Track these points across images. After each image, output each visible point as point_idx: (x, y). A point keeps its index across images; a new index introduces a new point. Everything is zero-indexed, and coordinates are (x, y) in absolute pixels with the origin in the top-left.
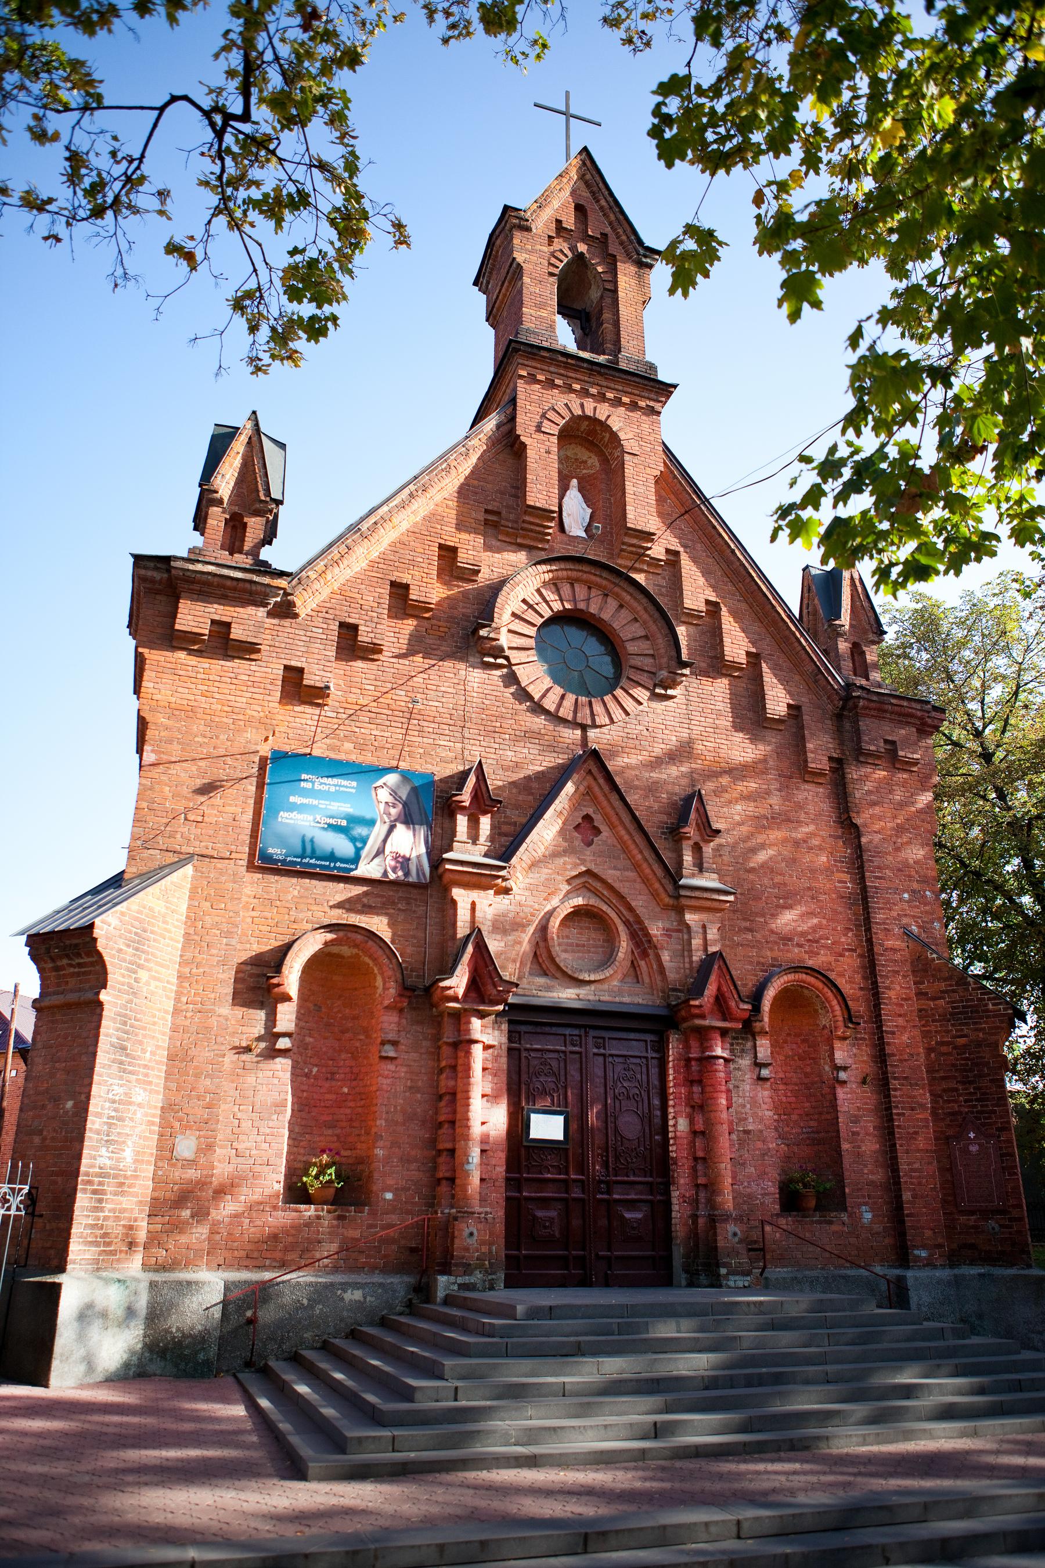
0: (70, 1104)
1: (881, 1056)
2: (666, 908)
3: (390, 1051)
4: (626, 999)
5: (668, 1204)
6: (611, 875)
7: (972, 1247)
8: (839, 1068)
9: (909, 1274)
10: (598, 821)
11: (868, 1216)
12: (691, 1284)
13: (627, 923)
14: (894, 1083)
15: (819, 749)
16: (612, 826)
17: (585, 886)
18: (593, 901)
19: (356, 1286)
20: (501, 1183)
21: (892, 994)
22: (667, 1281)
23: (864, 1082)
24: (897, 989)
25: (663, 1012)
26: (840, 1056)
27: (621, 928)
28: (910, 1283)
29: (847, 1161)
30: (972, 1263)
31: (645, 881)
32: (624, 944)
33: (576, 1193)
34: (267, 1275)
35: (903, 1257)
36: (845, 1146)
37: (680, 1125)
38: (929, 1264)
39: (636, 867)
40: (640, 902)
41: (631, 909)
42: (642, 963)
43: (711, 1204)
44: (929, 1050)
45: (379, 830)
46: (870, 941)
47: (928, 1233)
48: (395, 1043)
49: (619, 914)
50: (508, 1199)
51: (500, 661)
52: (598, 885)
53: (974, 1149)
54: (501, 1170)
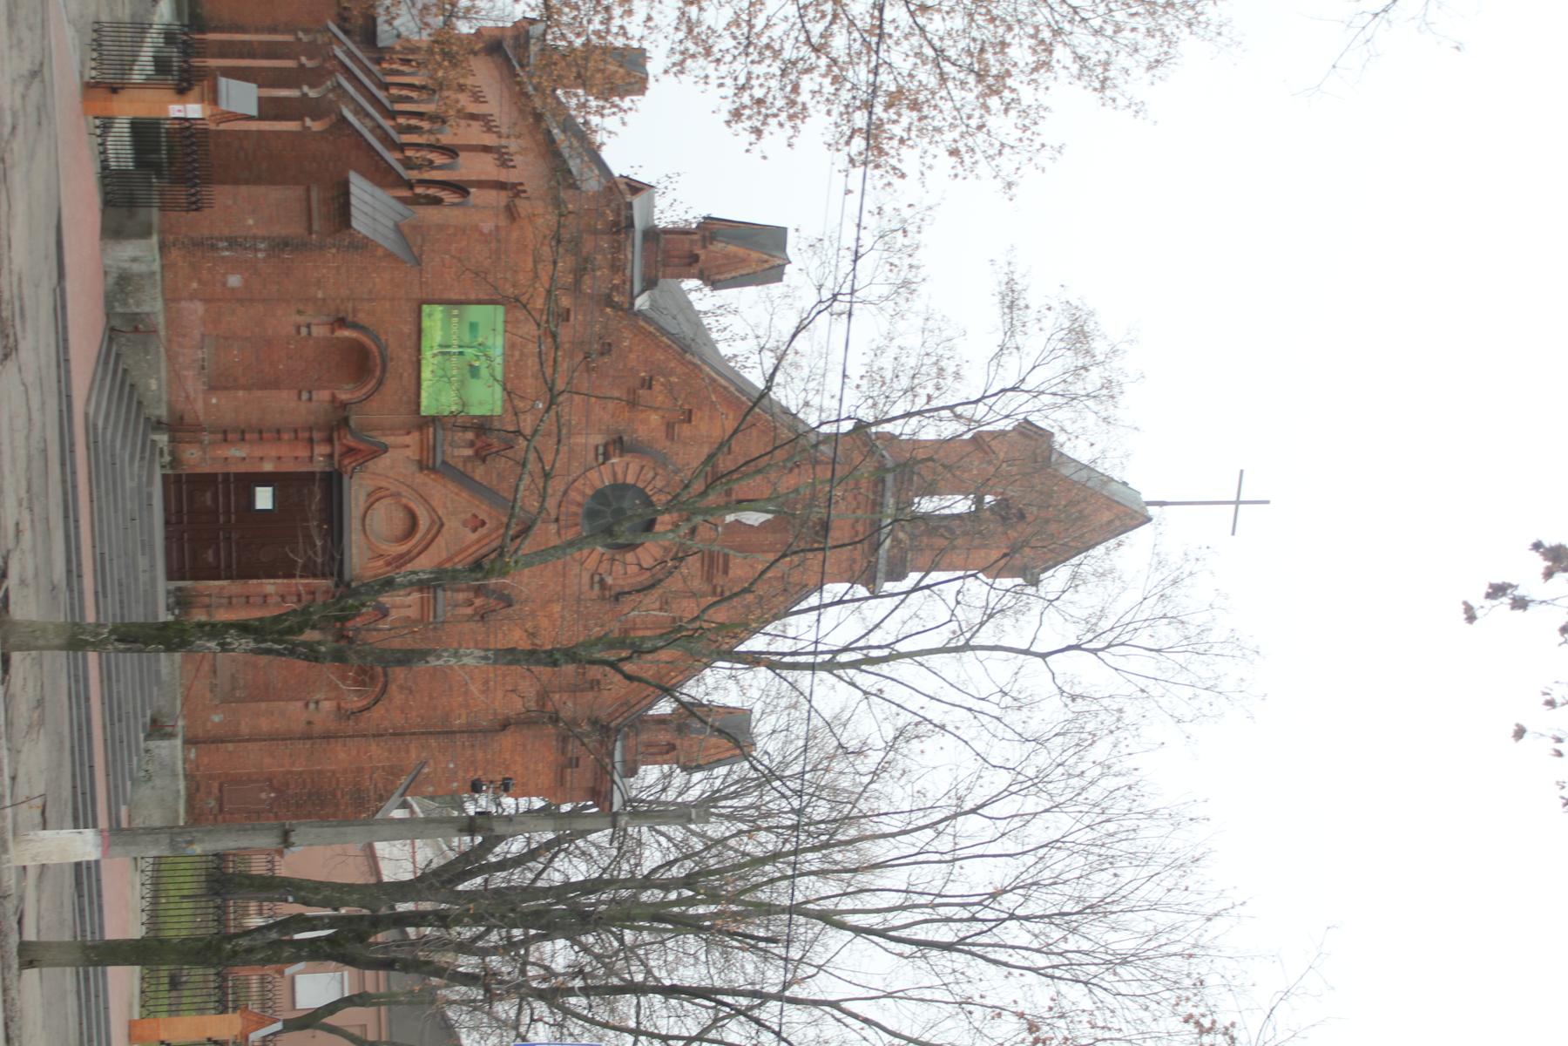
0: (251, 222)
3: (305, 396)
4: (354, 551)
5: (219, 578)
6: (441, 541)
7: (198, 790)
8: (317, 702)
9: (178, 742)
10: (482, 531)
11: (217, 718)
12: (168, 592)
13: (409, 552)
14: (308, 744)
16: (479, 541)
19: (159, 387)
20: (225, 470)
21: (374, 747)
22: (170, 576)
23: (309, 723)
25: (347, 577)
27: (404, 548)
28: (172, 742)
29: (253, 705)
30: (187, 789)
33: (222, 519)
34: (162, 333)
36: (263, 705)
38: (185, 760)
41: (420, 553)
42: (381, 562)
43: (219, 606)
44: (334, 772)
47: (206, 760)
48: (310, 399)
49: (415, 546)
50: (216, 475)
51: (601, 459)
52: (434, 531)
53: (263, 796)
54: (233, 469)
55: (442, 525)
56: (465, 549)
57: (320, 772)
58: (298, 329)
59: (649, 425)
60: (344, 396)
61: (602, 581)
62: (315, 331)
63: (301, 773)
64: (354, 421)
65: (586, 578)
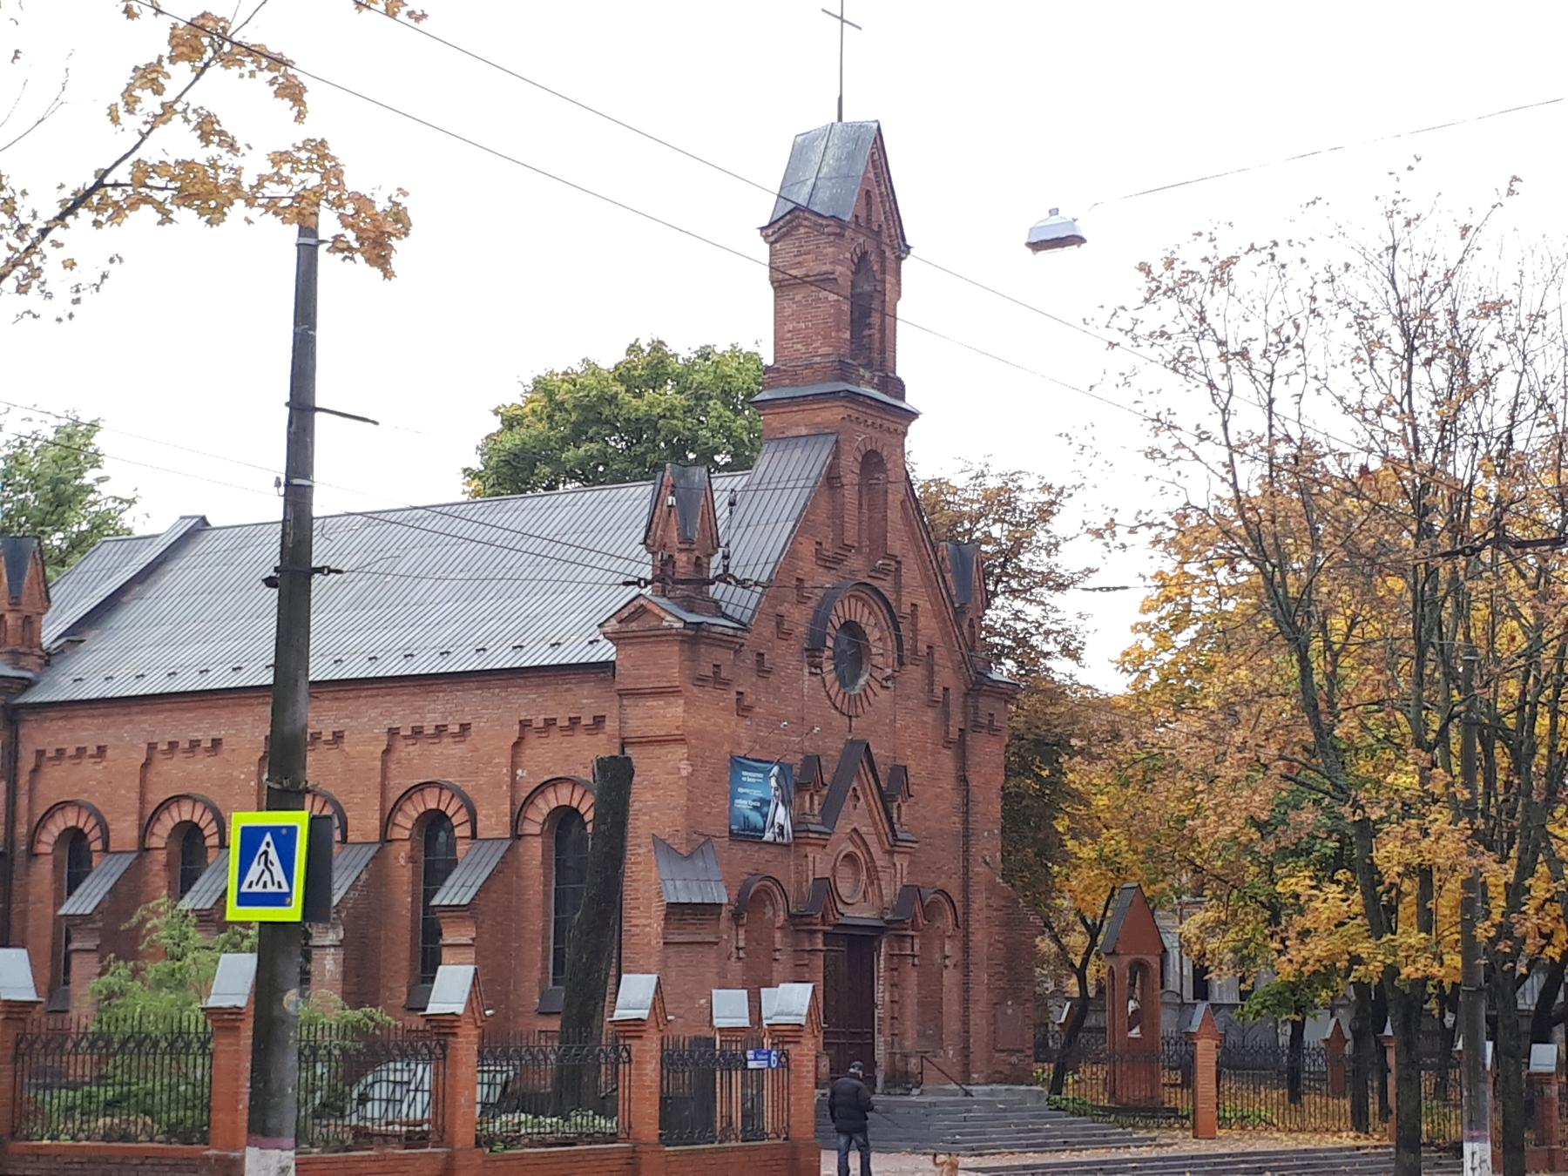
1: (966, 950)
2: (887, 852)
3: (778, 955)
6: (863, 830)
10: (859, 793)
14: (971, 967)
16: (866, 796)
18: (852, 848)
24: (979, 901)
25: (880, 924)
30: (1001, 1082)
31: (878, 835)
32: (864, 877)
35: (966, 1078)
37: (881, 994)
39: (875, 824)
40: (875, 849)
44: (990, 945)
45: (772, 806)
46: (966, 868)
53: (1010, 1011)
55: (855, 830)
56: (870, 811)
58: (739, 958)
59: (799, 617)
60: (781, 918)
61: (887, 679)
62: (741, 944)
63: (990, 976)
64: (793, 911)
65: (883, 694)
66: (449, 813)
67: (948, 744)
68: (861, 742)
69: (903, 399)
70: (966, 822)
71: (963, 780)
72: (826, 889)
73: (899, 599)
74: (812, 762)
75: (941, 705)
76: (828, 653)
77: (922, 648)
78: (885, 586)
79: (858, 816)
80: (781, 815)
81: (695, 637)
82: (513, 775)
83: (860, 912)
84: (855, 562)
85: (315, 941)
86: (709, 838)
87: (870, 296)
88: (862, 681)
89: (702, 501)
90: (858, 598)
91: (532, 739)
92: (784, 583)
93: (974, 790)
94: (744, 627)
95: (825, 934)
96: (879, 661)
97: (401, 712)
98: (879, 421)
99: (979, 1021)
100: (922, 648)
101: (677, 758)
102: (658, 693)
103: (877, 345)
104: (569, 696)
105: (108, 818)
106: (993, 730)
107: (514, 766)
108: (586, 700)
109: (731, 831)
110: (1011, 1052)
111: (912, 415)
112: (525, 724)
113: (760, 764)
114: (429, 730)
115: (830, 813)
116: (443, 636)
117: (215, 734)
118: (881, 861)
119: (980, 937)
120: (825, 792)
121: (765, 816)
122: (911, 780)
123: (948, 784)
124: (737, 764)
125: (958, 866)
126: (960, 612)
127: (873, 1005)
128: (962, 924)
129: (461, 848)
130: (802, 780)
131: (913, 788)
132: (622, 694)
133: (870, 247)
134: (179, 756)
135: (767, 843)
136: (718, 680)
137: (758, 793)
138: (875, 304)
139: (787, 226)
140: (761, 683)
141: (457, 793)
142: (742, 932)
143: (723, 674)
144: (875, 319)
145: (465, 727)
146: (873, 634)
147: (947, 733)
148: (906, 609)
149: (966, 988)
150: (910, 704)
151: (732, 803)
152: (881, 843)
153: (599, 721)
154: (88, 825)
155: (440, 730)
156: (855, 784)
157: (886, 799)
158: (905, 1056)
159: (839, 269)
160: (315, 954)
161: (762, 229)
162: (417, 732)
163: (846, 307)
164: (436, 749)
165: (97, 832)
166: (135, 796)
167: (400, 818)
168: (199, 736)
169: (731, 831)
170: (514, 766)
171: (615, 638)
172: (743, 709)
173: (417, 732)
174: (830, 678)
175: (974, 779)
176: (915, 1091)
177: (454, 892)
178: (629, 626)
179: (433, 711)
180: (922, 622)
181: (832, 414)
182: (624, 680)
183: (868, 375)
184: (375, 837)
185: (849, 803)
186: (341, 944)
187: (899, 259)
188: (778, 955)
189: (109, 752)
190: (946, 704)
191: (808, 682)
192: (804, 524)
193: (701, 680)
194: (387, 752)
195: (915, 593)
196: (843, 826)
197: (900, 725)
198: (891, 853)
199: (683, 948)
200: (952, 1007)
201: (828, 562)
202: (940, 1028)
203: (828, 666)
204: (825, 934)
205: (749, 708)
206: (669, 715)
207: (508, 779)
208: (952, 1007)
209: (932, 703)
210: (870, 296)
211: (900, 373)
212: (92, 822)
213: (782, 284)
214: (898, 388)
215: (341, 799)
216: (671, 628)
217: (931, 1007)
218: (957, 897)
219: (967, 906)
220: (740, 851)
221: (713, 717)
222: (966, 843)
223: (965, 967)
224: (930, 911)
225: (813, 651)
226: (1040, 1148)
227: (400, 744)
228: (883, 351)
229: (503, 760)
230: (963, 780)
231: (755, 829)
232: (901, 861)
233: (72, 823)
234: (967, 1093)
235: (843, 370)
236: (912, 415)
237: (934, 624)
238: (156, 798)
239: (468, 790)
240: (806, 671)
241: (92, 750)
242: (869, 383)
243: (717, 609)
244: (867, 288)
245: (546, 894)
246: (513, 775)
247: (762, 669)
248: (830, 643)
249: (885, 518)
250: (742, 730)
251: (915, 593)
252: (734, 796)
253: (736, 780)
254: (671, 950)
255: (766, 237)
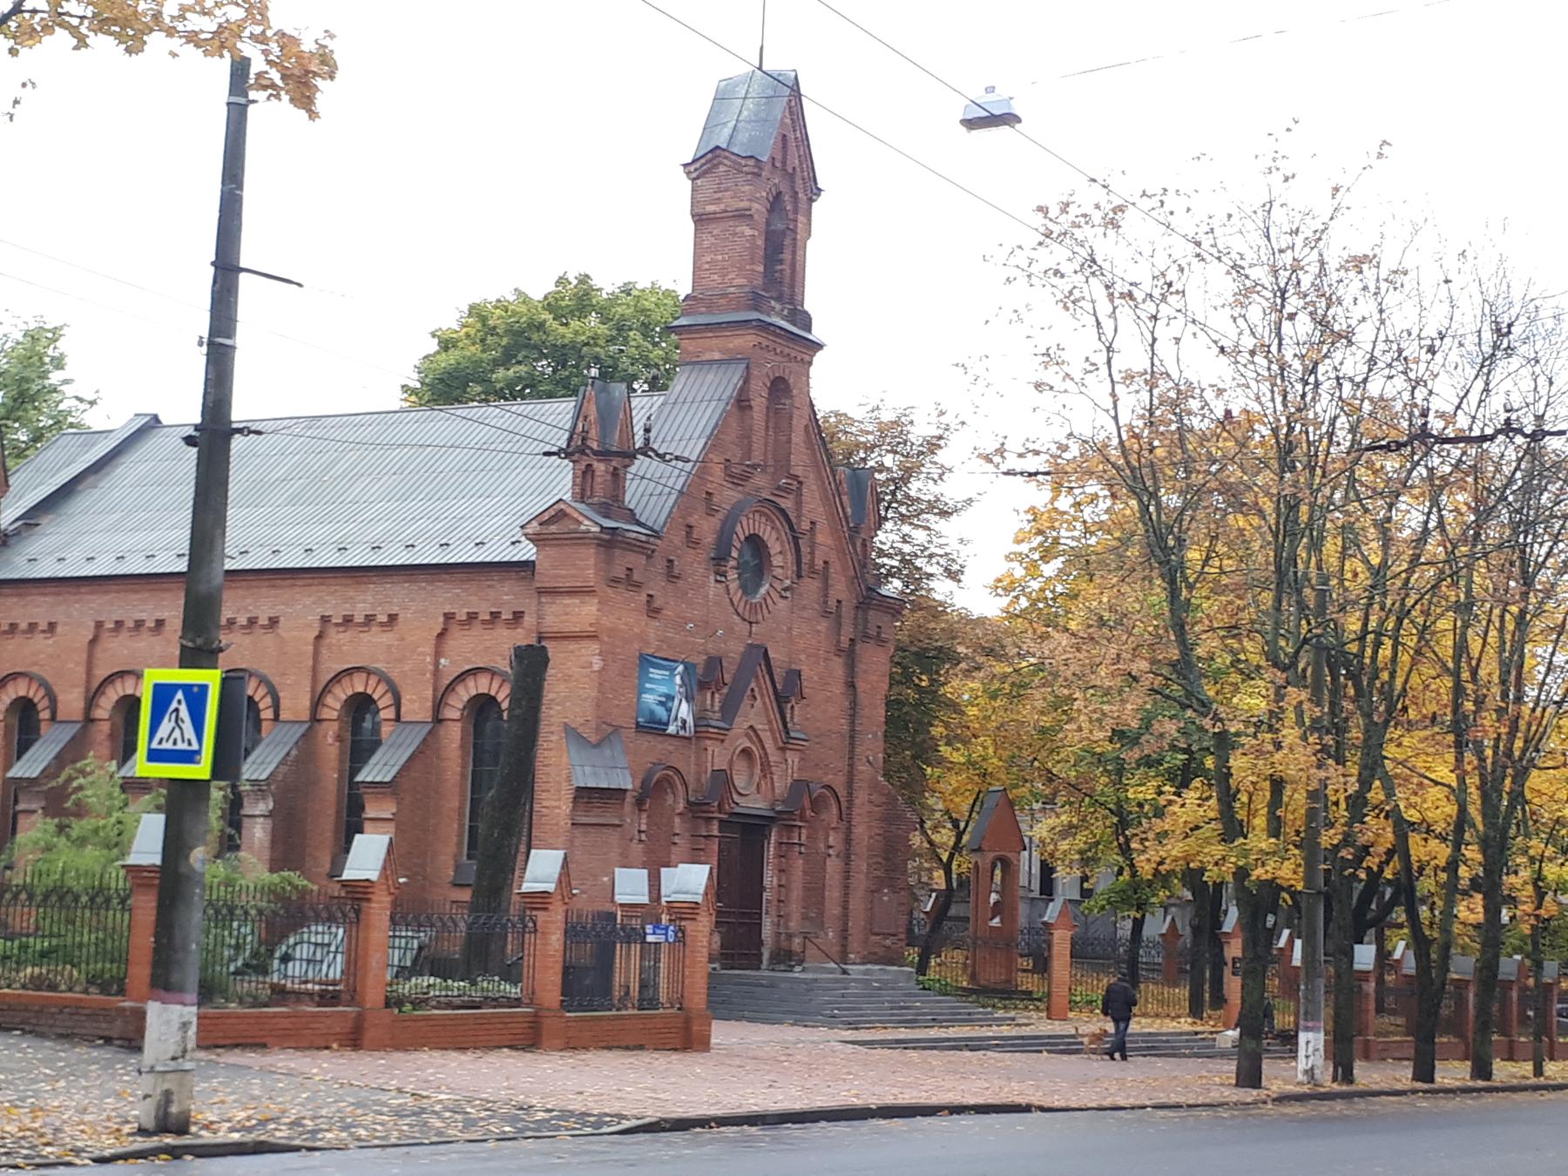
1: (848, 841)
3: (676, 839)
15: (847, 631)
16: (762, 696)
17: (747, 735)
18: (748, 744)
24: (861, 797)
25: (772, 814)
26: (831, 841)
30: (876, 963)
31: (771, 730)
32: (758, 770)
35: (843, 958)
37: (770, 878)
39: (770, 722)
40: (769, 745)
41: (763, 748)
45: (676, 702)
56: (766, 709)
57: (869, 850)
59: (707, 529)
60: (681, 806)
61: (785, 589)
62: (644, 828)
64: (692, 799)
65: (782, 604)
66: (375, 697)
67: (839, 651)
68: (758, 646)
69: (809, 331)
70: (853, 723)
71: (851, 686)
72: (723, 779)
73: (799, 517)
74: (714, 663)
75: (832, 614)
76: (732, 563)
77: (819, 563)
78: (787, 504)
79: (755, 714)
80: (684, 710)
81: (610, 542)
82: (436, 664)
83: (753, 802)
84: (760, 480)
85: (247, 810)
86: (617, 729)
87: (783, 233)
88: (763, 591)
89: (621, 415)
90: (762, 514)
91: (455, 630)
92: (696, 495)
93: (861, 696)
94: (657, 535)
95: (721, 821)
96: (778, 572)
97: (334, 602)
98: (787, 350)
99: (857, 904)
100: (819, 563)
101: (590, 654)
102: (572, 592)
103: (787, 280)
104: (491, 592)
105: (56, 690)
106: (881, 642)
107: (438, 654)
108: (507, 595)
109: (637, 724)
110: (887, 935)
111: (819, 346)
112: (449, 617)
113: (668, 662)
114: (359, 619)
115: (729, 710)
116: (376, 532)
117: (159, 615)
118: (774, 757)
119: (860, 831)
120: (725, 690)
121: (669, 710)
122: (805, 684)
123: (837, 689)
124: (646, 661)
125: (843, 764)
126: (855, 530)
127: (762, 888)
128: (845, 817)
129: (386, 729)
130: (704, 679)
131: (806, 691)
132: (541, 592)
133: (784, 188)
134: (124, 634)
135: (671, 735)
136: (630, 582)
137: (663, 689)
138: (787, 241)
139: (706, 165)
140: (670, 587)
141: (383, 678)
142: (644, 815)
143: (636, 577)
144: (787, 256)
145: (393, 618)
146: (774, 547)
147: (839, 642)
148: (805, 526)
149: (847, 874)
150: (805, 614)
151: (639, 698)
152: (775, 739)
153: (518, 616)
154: (36, 694)
155: (369, 619)
156: (753, 685)
157: (781, 700)
158: (790, 936)
159: (756, 206)
160: (246, 822)
161: (685, 165)
162: (348, 620)
163: (760, 242)
164: (365, 637)
165: (45, 702)
166: (82, 670)
167: (329, 700)
168: (143, 616)
169: (637, 724)
170: (438, 654)
171: (536, 539)
172: (653, 611)
173: (348, 620)
174: (734, 586)
175: (861, 686)
176: (798, 969)
177: (376, 770)
178: (550, 528)
179: (363, 601)
180: (820, 538)
181: (745, 341)
182: (542, 580)
183: (778, 307)
184: (306, 716)
185: (747, 701)
186: (269, 815)
187: (811, 201)
188: (676, 839)
189: (59, 629)
190: (839, 616)
191: (713, 589)
192: (715, 442)
193: (615, 581)
194: (319, 637)
195: (813, 508)
196: (741, 724)
197: (796, 632)
198: (783, 749)
199: (590, 829)
200: (833, 894)
201: (738, 478)
202: (821, 914)
203: (733, 575)
204: (721, 821)
205: (658, 610)
206: (584, 612)
207: (431, 667)
208: (833, 894)
209: (826, 614)
210: (783, 233)
211: (807, 306)
212: (42, 692)
213: (701, 219)
214: (807, 323)
215: (275, 680)
216: (589, 532)
217: (814, 892)
218: (842, 793)
219: (850, 802)
220: (646, 742)
221: (626, 616)
222: (852, 745)
223: (847, 858)
224: (817, 804)
225: (719, 560)
226: (911, 1023)
227: (332, 631)
228: (792, 286)
229: (428, 649)
230: (851, 686)
231: (660, 722)
232: (793, 758)
233: (22, 693)
234: (845, 972)
235: (756, 301)
236: (819, 346)
237: (830, 542)
238: (101, 673)
239: (394, 675)
240: (712, 578)
241: (43, 626)
242: (779, 314)
243: (631, 516)
244: (780, 226)
245: (463, 776)
246: (436, 664)
247: (672, 576)
248: (735, 554)
249: (789, 441)
250: (653, 629)
251: (813, 508)
252: (641, 691)
253: (644, 676)
254: (578, 832)
255: (688, 174)
